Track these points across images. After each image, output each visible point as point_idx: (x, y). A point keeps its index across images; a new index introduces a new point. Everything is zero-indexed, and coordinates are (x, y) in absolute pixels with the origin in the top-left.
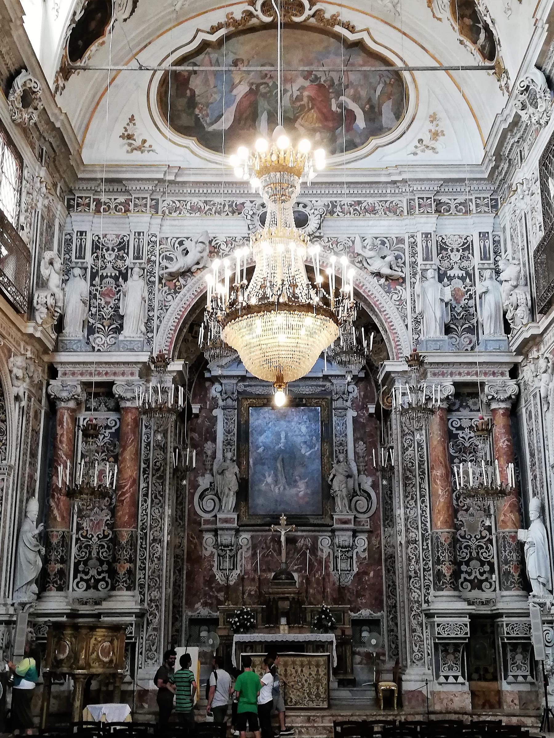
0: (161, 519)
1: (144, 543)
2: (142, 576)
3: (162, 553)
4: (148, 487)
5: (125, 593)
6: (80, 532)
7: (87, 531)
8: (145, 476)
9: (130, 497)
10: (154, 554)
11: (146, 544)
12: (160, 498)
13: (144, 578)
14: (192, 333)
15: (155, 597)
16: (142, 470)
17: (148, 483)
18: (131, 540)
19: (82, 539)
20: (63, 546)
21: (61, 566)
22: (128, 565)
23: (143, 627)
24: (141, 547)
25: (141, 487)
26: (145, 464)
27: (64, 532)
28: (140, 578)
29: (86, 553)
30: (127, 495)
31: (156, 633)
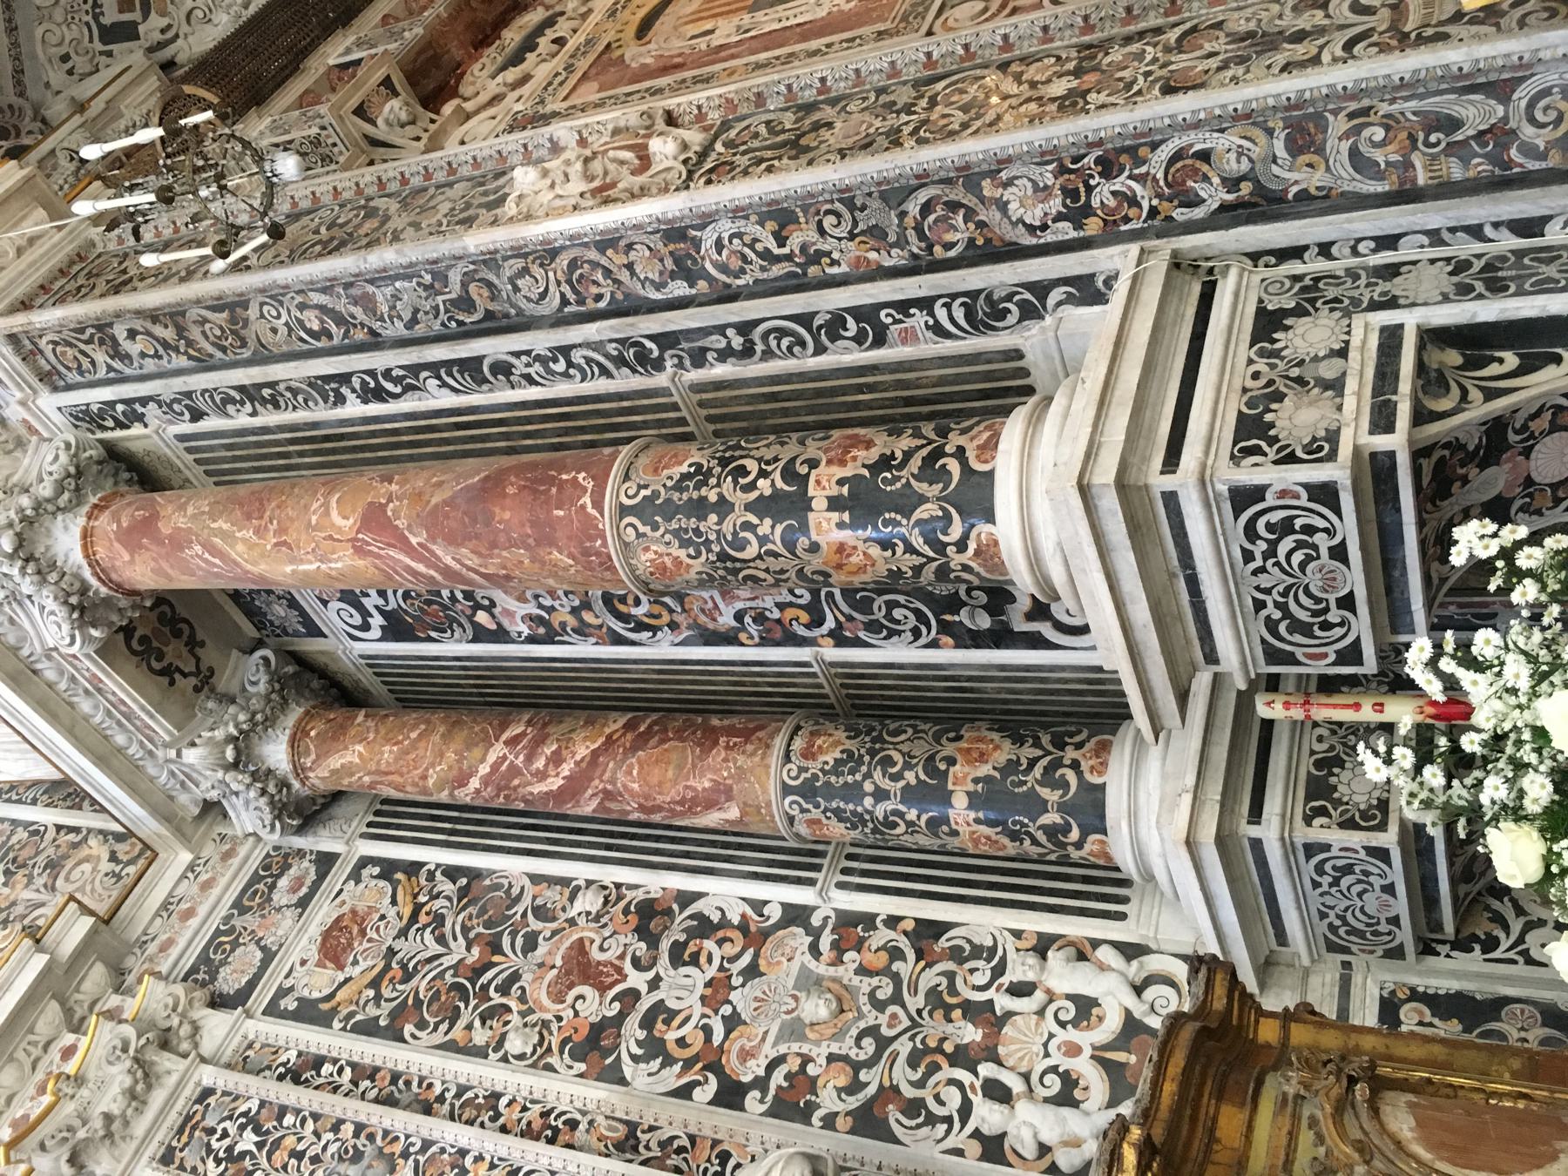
0: (554, 253)
1: (718, 342)
2: (919, 319)
3: (738, 212)
4: (434, 367)
5: (1006, 528)
6: (801, 631)
7: (781, 606)
8: (389, 386)
9: (452, 540)
10: (766, 255)
11: (721, 330)
12: (455, 277)
13: (926, 304)
14: (134, 24)
15: (1042, 191)
16: (375, 409)
17: (415, 369)
18: (669, 510)
19: (830, 623)
20: (853, 791)
21: (960, 801)
22: (827, 528)
23: (1296, 252)
24: (747, 352)
25: (448, 400)
26: (340, 400)
27: (786, 790)
28: (938, 330)
29: (891, 605)
30: (449, 560)
31: (1338, 125)
